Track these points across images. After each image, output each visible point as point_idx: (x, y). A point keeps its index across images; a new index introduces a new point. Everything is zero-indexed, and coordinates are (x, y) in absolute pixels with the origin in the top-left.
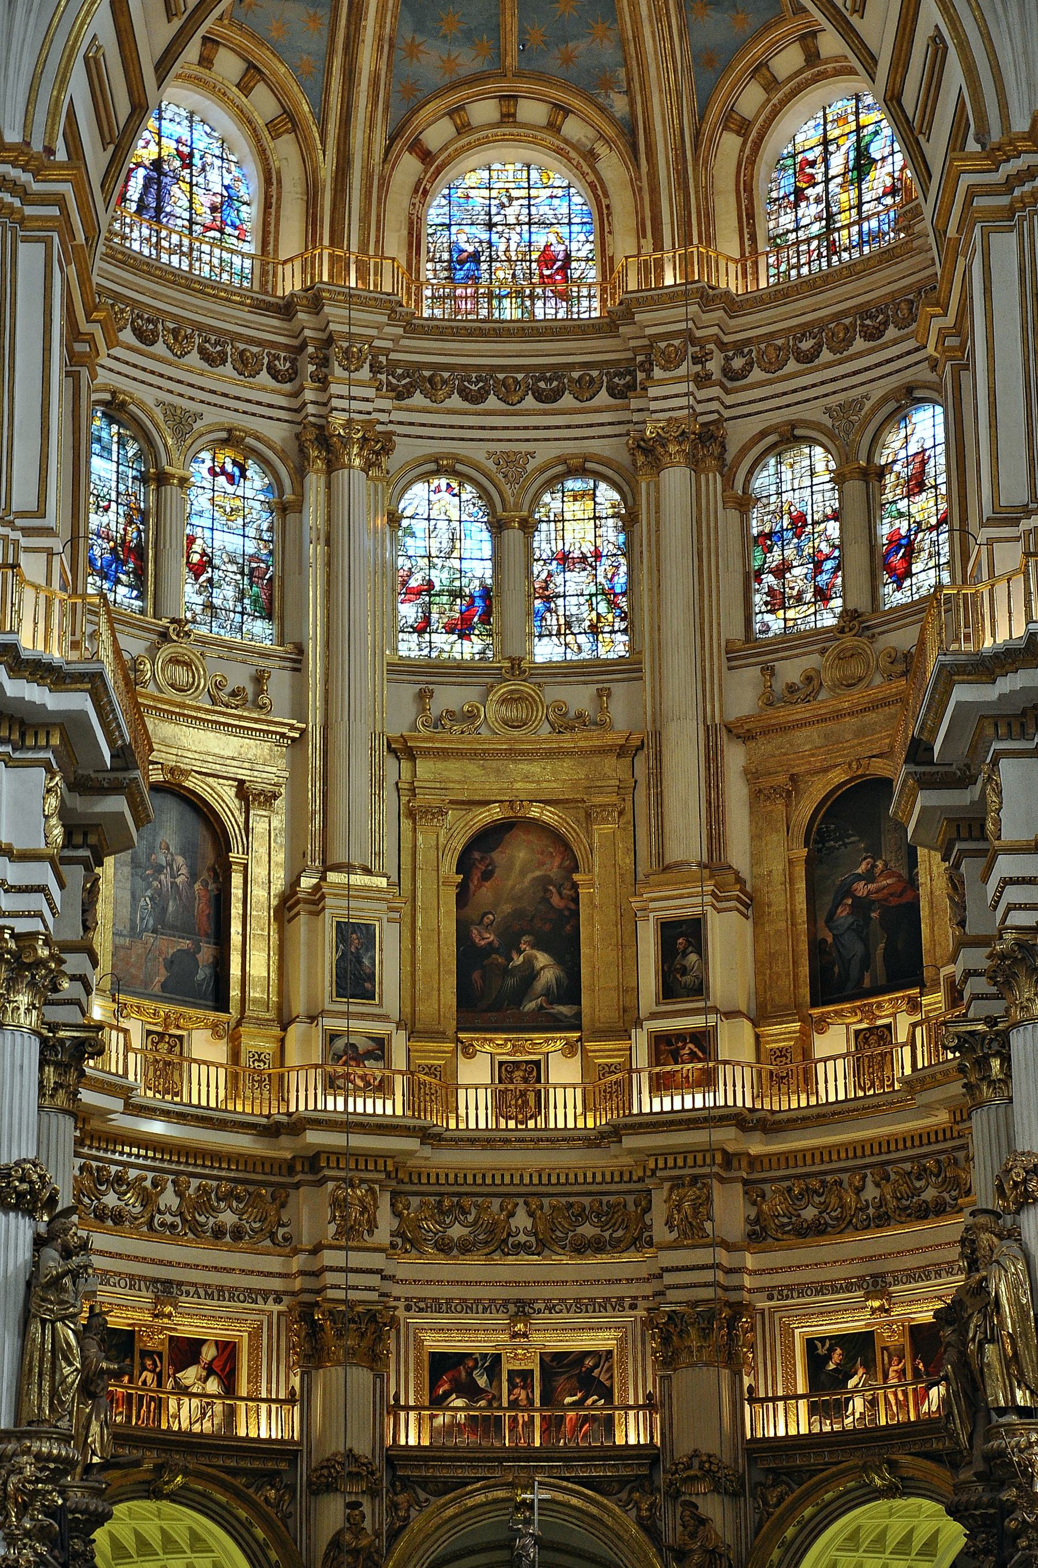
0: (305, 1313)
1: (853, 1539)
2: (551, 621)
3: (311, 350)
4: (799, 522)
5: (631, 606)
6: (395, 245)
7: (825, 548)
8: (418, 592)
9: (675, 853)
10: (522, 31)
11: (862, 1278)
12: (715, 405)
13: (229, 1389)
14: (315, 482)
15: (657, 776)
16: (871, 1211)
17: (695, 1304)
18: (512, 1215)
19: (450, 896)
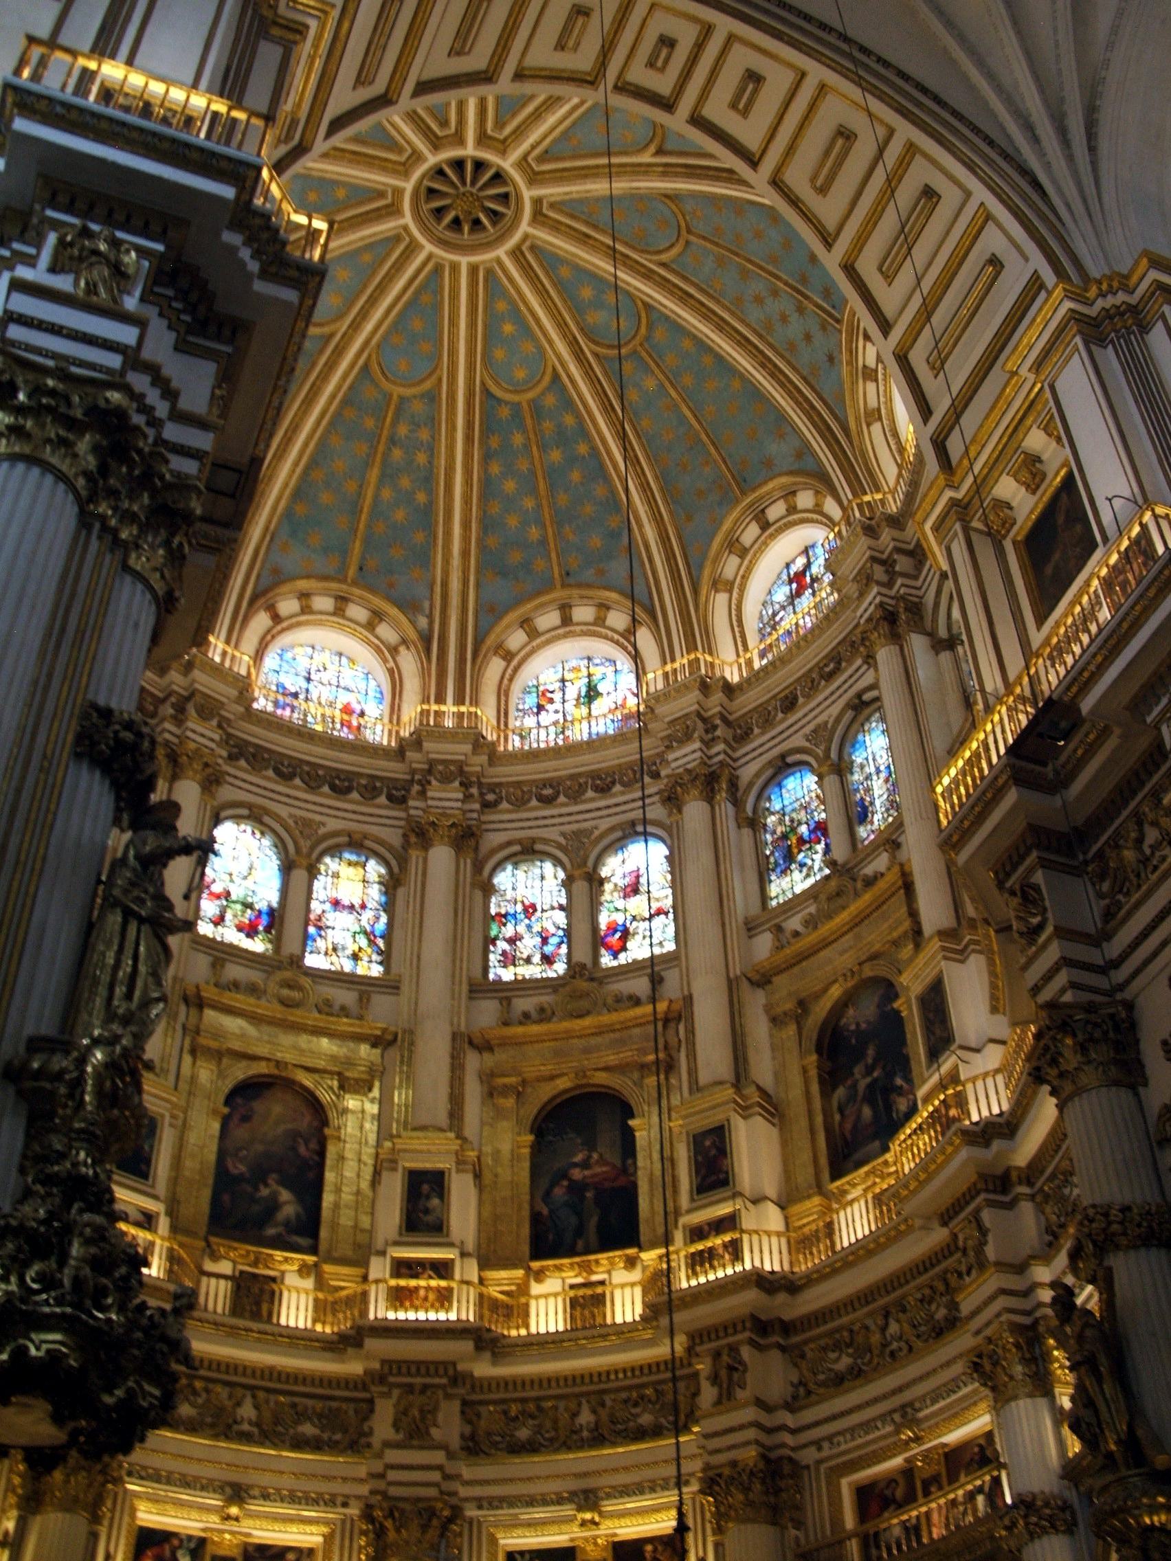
2: (321, 944)
3: (173, 699)
4: (530, 910)
5: (388, 944)
7: (552, 930)
8: (218, 897)
10: (363, 558)
11: (573, 1494)
12: (475, 815)
15: (408, 1060)
16: (585, 1434)
17: (419, 1500)
18: (239, 1404)
19: (216, 1126)
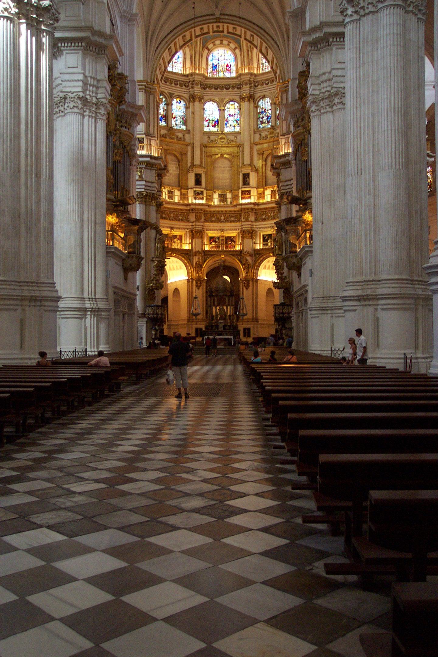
0: (192, 231)
1: (269, 261)
2: (228, 125)
6: (204, 66)
7: (269, 115)
8: (207, 120)
9: (245, 163)
13: (181, 242)
14: (191, 104)
15: (243, 151)
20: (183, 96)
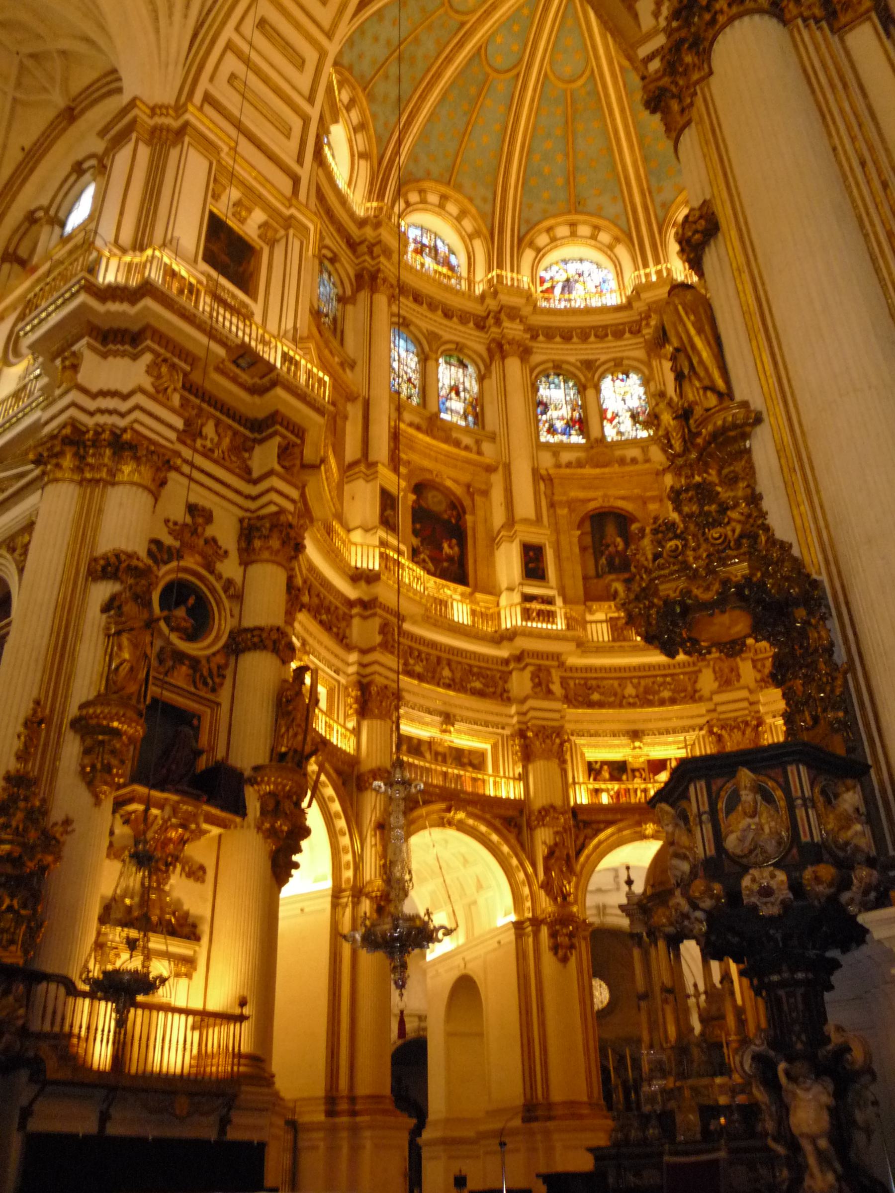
20: (628, 358)
